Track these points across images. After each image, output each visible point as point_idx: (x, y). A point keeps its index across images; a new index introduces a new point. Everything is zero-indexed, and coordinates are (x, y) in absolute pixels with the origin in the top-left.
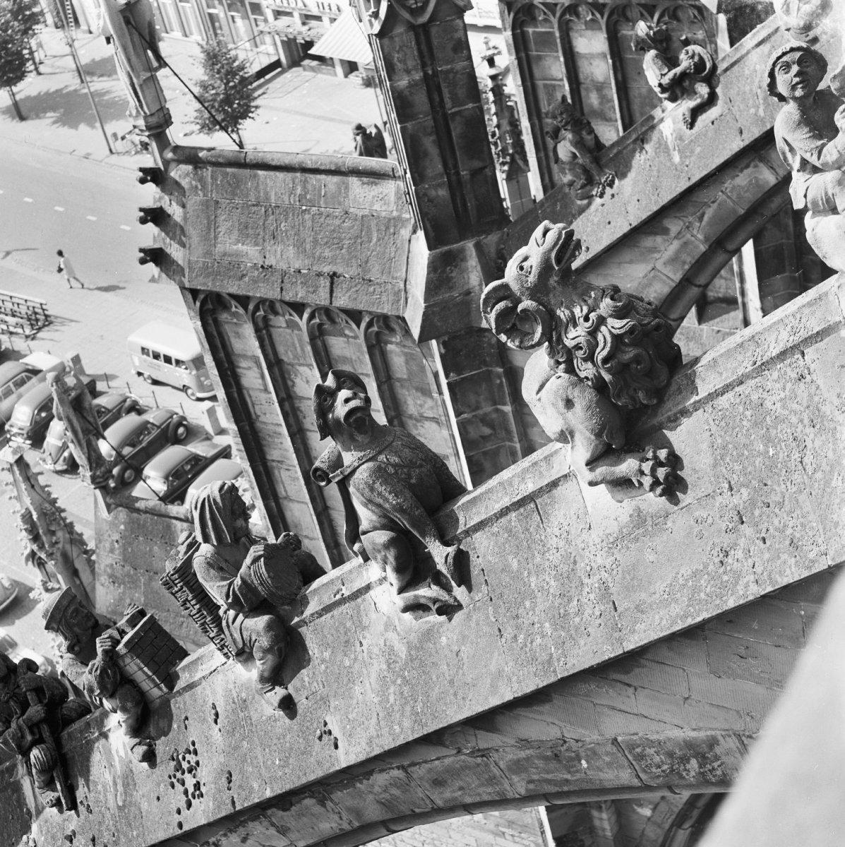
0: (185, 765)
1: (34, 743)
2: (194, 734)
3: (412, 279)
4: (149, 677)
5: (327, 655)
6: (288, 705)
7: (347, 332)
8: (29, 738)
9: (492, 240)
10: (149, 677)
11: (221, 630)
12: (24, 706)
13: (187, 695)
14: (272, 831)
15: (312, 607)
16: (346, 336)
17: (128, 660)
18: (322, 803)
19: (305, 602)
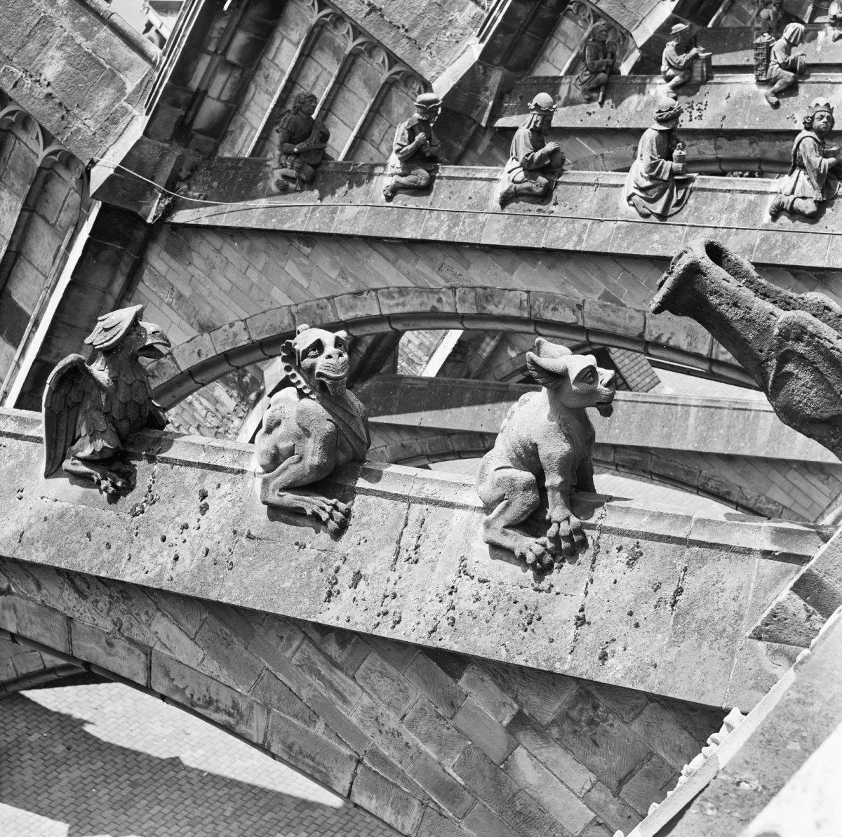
0: (695, 108)
1: (604, 72)
2: (709, 99)
3: (648, 20)
4: (702, 72)
5: (807, 96)
6: (776, 106)
7: (580, 22)
8: (604, 68)
9: (697, 28)
10: (702, 72)
11: (767, 67)
12: (605, 57)
13: (713, 86)
14: (712, 147)
15: (811, 79)
16: (577, 24)
17: (699, 62)
18: (751, 143)
19: (808, 77)
